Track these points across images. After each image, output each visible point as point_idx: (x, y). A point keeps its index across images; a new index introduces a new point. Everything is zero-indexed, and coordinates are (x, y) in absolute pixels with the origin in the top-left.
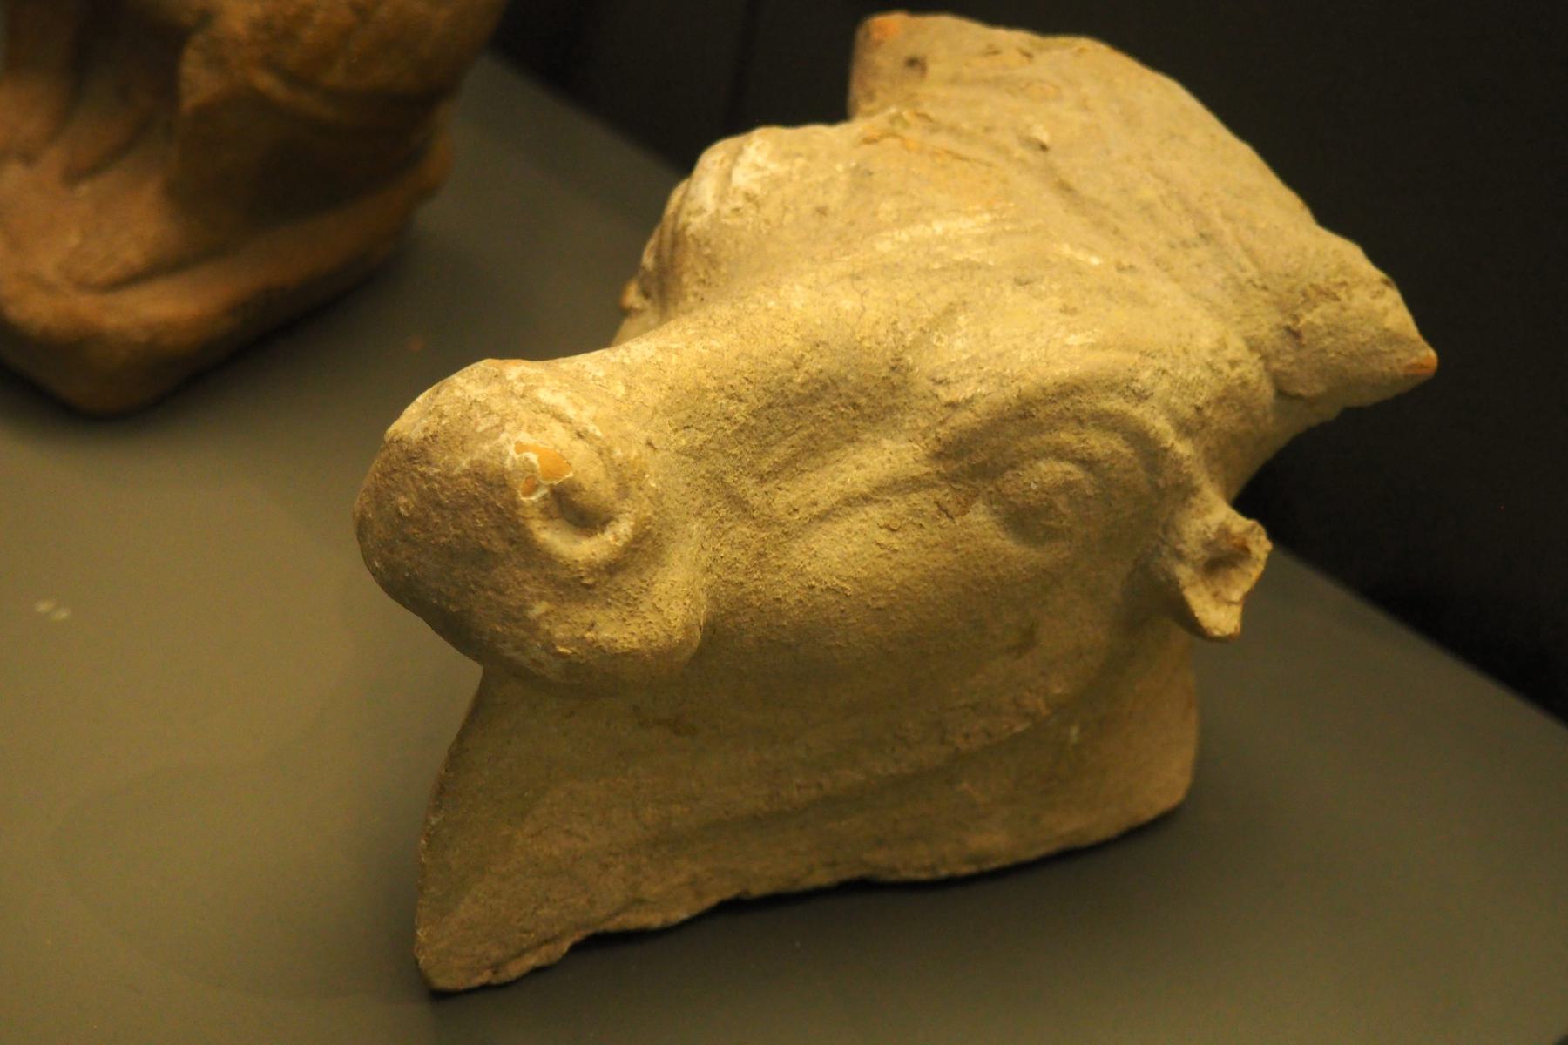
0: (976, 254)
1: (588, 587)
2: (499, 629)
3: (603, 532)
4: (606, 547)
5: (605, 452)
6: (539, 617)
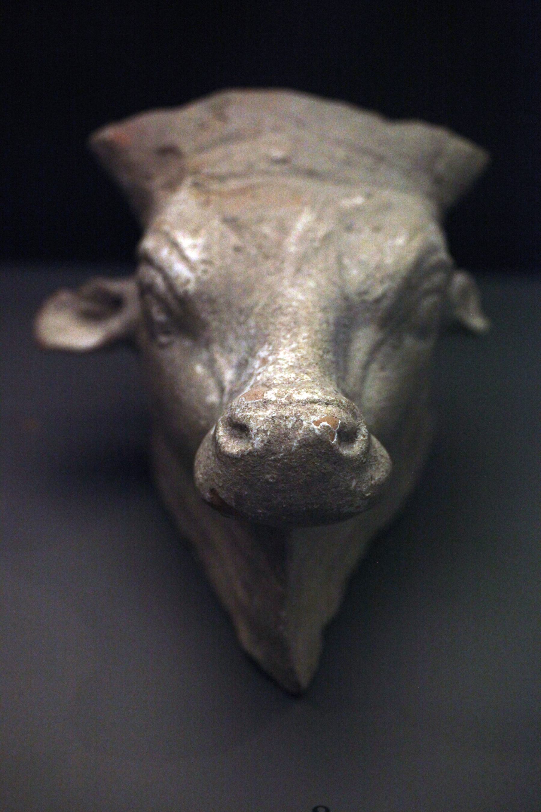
0: (322, 230)
1: (365, 463)
2: (340, 503)
3: (356, 437)
4: (363, 442)
5: (340, 404)
6: (355, 487)
